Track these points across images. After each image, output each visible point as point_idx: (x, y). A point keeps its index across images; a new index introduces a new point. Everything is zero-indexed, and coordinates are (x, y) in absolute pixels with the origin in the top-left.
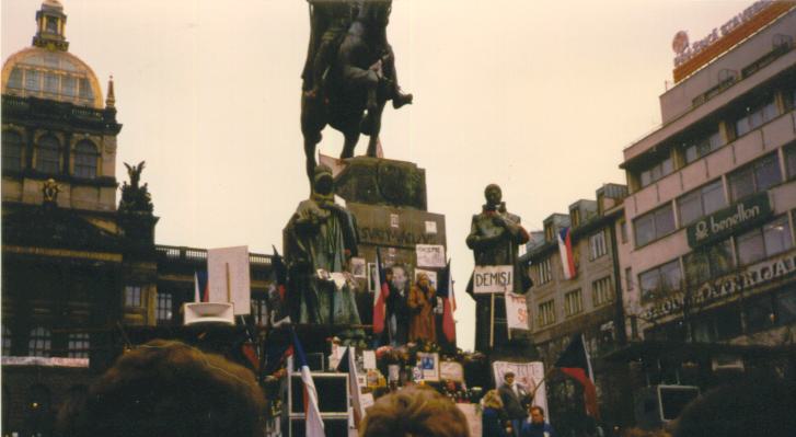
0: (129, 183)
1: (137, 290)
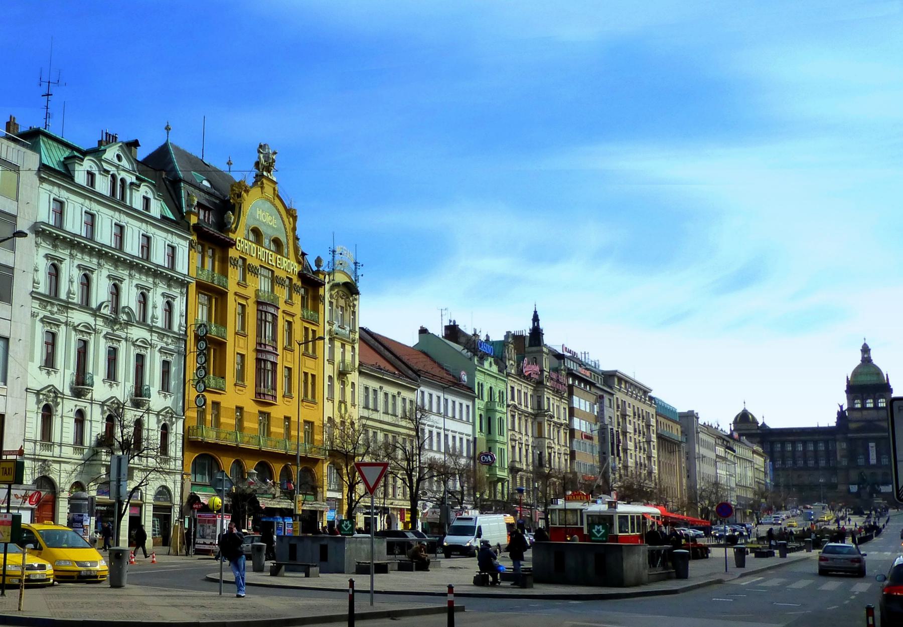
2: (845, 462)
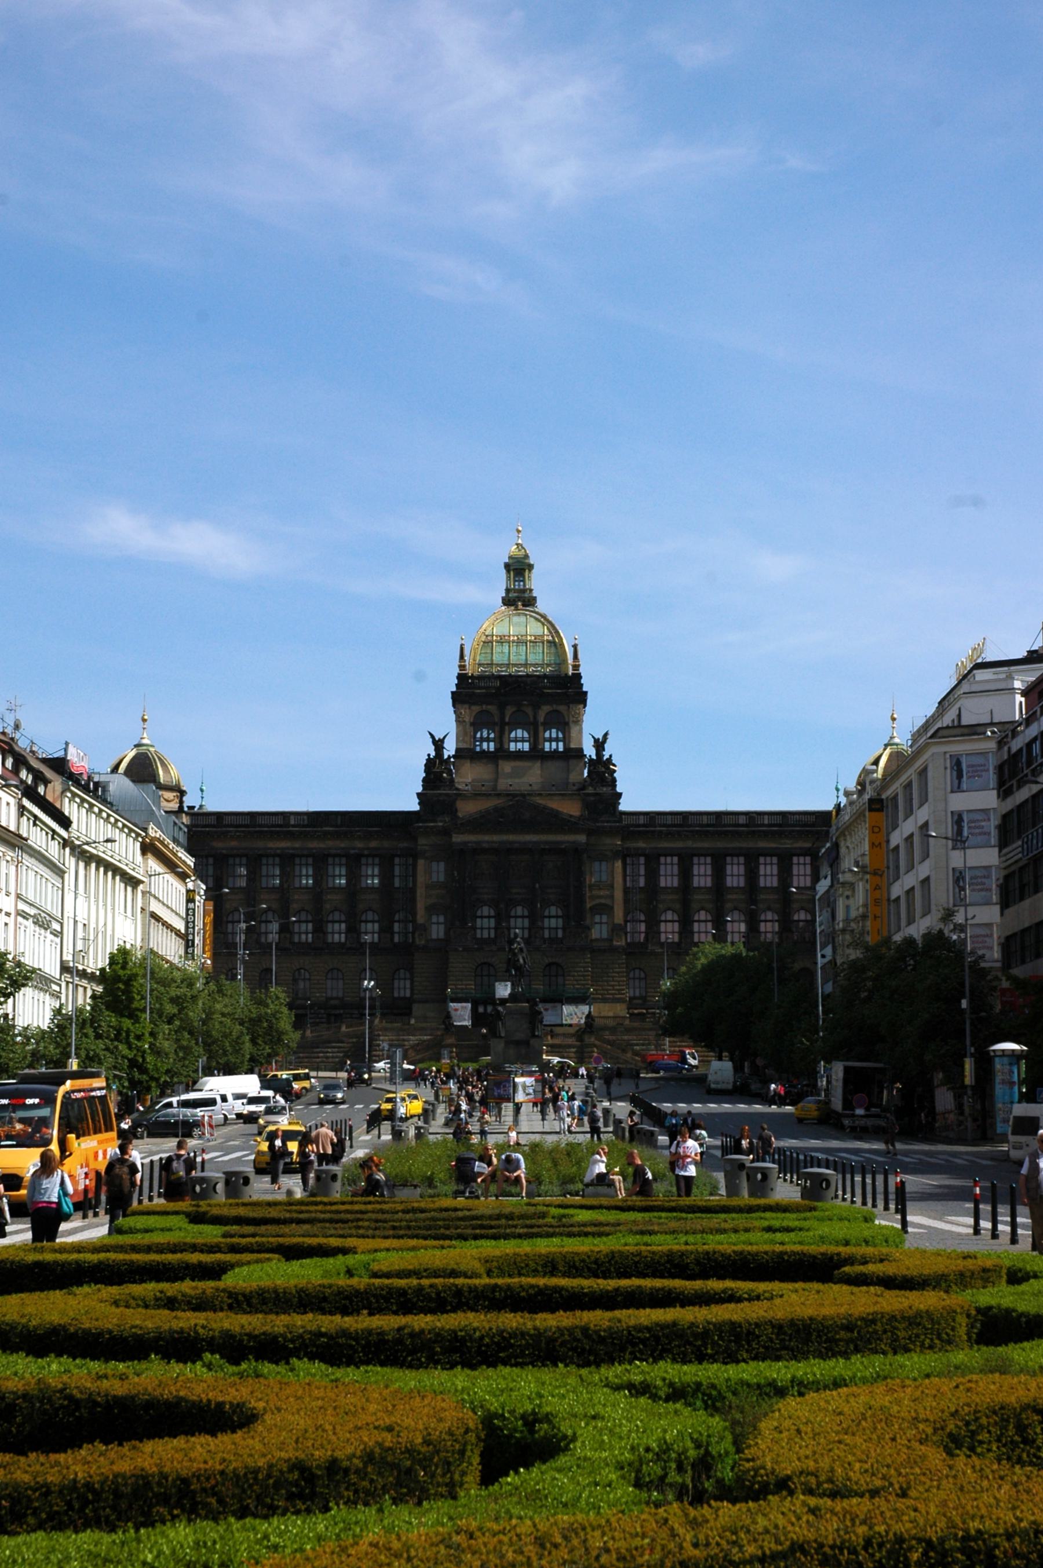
0: (594, 757)
1: (604, 864)
2: (437, 931)
